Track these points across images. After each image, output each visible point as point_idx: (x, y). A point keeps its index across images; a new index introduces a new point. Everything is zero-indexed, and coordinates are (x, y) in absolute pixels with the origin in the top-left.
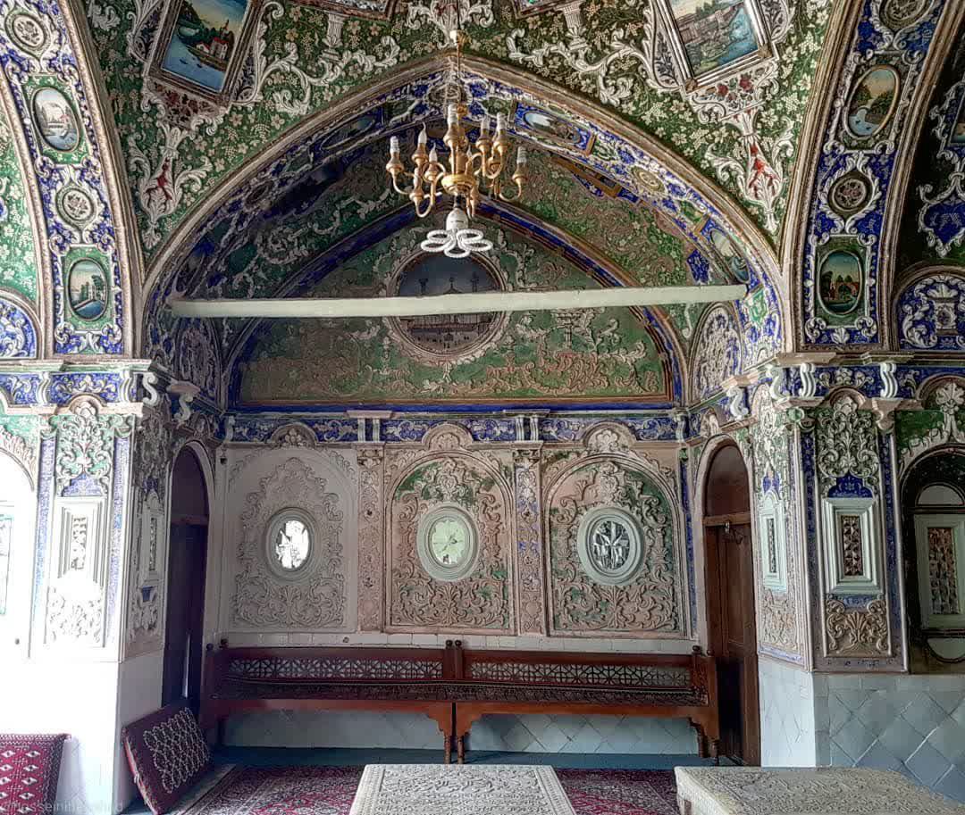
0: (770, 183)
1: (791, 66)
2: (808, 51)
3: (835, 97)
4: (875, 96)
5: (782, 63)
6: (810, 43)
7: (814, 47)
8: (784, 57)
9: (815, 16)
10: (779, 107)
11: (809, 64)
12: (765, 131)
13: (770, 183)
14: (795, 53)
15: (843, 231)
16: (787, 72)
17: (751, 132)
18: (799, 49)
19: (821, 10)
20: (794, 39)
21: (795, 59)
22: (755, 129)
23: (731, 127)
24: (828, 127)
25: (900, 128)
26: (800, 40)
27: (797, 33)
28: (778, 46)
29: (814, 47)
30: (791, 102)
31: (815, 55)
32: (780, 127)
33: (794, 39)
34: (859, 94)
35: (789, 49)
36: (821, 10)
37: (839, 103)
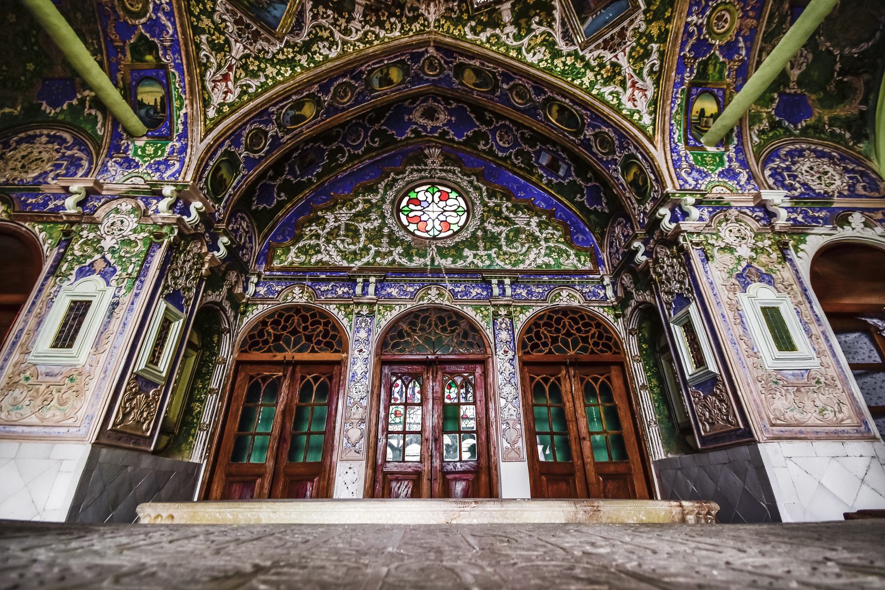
0: (226, 93)
1: (285, 57)
2: (300, 60)
3: (295, 94)
4: (302, 113)
5: (281, 50)
6: (303, 60)
7: (304, 63)
8: (285, 50)
9: (315, 53)
10: (262, 65)
11: (295, 66)
12: (245, 67)
13: (226, 93)
14: (292, 55)
15: (240, 154)
16: (281, 57)
17: (237, 57)
18: (295, 56)
19: (321, 54)
20: (296, 49)
21: (289, 57)
22: (240, 59)
23: (227, 41)
24: (281, 101)
25: (293, 137)
26: (299, 52)
27: (300, 48)
28: (287, 42)
29: (304, 63)
30: (271, 71)
31: (302, 66)
32: (254, 75)
33: (296, 49)
34: (299, 105)
35: (290, 50)
36: (321, 54)
37: (294, 97)
